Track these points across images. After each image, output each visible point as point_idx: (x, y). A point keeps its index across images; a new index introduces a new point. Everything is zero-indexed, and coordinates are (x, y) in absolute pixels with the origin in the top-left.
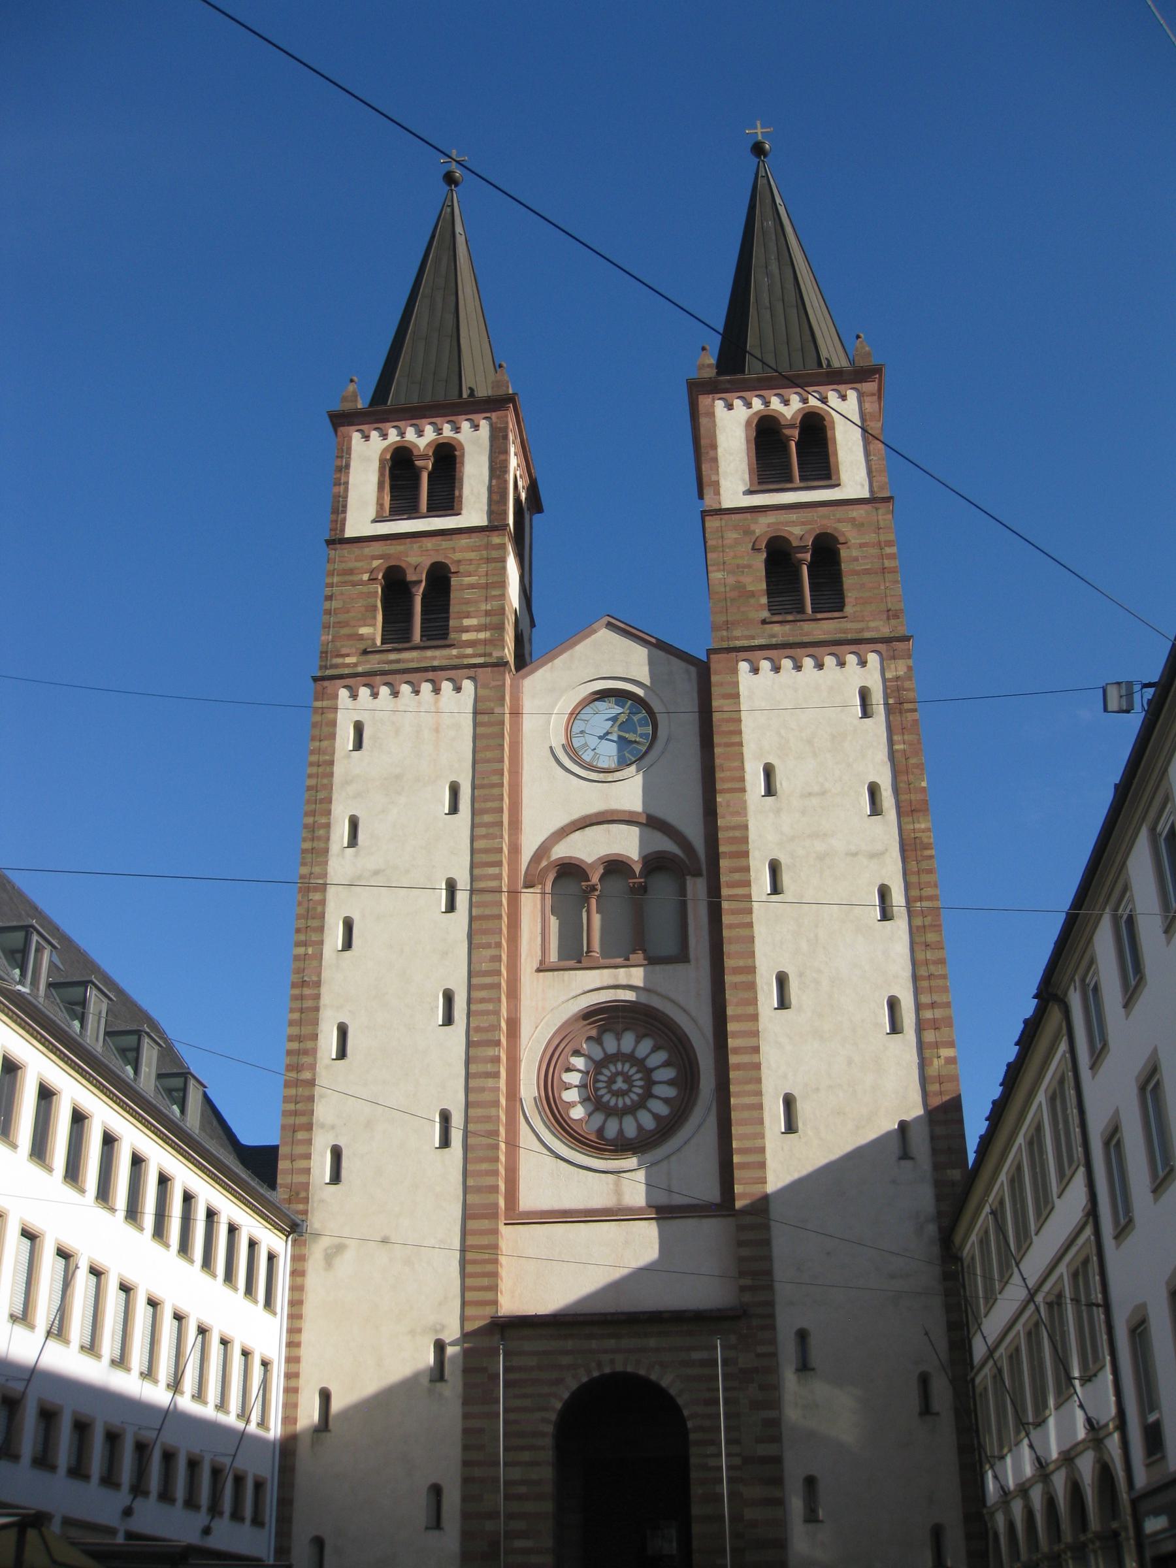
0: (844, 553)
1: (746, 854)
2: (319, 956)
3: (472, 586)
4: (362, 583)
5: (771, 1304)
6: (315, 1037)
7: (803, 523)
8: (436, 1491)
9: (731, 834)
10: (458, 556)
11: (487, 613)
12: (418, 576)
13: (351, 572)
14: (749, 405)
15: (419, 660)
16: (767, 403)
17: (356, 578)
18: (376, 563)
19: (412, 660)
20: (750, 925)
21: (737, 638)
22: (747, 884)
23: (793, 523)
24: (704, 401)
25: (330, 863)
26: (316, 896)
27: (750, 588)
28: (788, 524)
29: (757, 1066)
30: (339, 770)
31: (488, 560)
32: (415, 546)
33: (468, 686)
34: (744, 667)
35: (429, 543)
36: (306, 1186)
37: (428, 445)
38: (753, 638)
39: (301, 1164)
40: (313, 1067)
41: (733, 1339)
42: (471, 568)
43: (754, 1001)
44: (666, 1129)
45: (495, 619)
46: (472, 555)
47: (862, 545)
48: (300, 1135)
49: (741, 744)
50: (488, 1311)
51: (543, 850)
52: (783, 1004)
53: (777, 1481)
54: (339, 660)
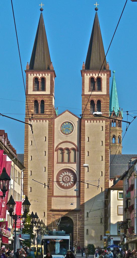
0: (101, 103)
2: (27, 161)
3: (48, 104)
4: (31, 102)
6: (27, 172)
7: (96, 98)
9: (83, 147)
10: (45, 99)
11: (50, 109)
12: (39, 102)
15: (40, 116)
16: (93, 75)
17: (30, 101)
18: (33, 99)
19: (39, 116)
21: (85, 117)
24: (83, 74)
25: (29, 148)
26: (27, 152)
31: (50, 100)
32: (39, 96)
33: (47, 121)
34: (86, 121)
35: (41, 96)
38: (87, 117)
39: (26, 189)
40: (27, 176)
41: (79, 213)
42: (47, 101)
43: (84, 171)
44: (73, 185)
45: (51, 110)
46: (48, 99)
47: (104, 102)
48: (26, 186)
50: (50, 208)
51: (57, 146)
53: (84, 230)
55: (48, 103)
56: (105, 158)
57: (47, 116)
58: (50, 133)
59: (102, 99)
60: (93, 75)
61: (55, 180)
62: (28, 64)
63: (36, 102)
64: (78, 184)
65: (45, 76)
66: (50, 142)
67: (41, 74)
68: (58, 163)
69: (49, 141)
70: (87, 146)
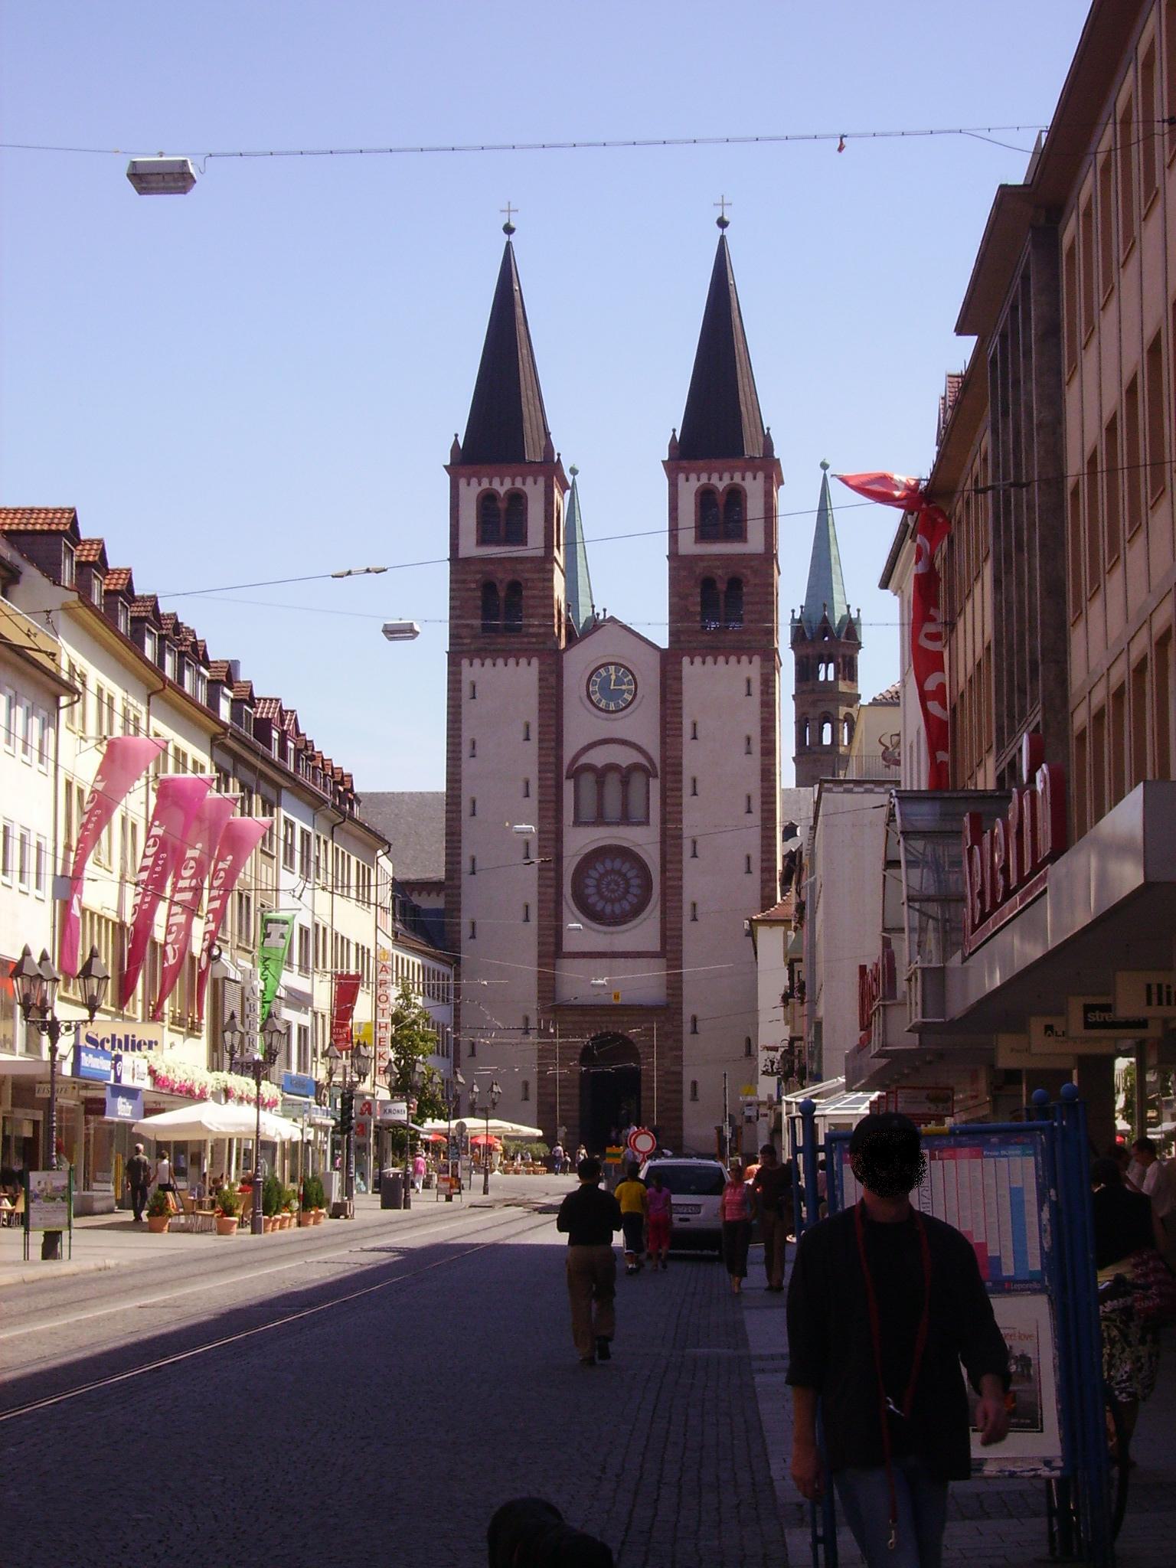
1: (680, 773)
3: (534, 597)
5: (681, 1003)
6: (459, 863)
8: (526, 1085)
10: (527, 575)
11: (544, 616)
13: (464, 582)
14: (699, 480)
16: (709, 479)
20: (681, 813)
22: (680, 790)
23: (718, 568)
27: (692, 609)
28: (718, 568)
29: (681, 887)
30: (464, 710)
33: (535, 661)
34: (686, 660)
36: (459, 940)
37: (506, 493)
46: (536, 576)
47: (755, 585)
49: (681, 708)
52: (695, 856)
53: (680, 1082)
54: (460, 641)
55: (535, 592)
56: (763, 803)
57: (533, 643)
58: (546, 707)
59: (748, 572)
60: (709, 479)
61: (567, 890)
62: (456, 441)
63: (489, 588)
64: (657, 903)
65: (523, 488)
66: (545, 745)
67: (508, 484)
68: (578, 822)
69: (540, 741)
70: (693, 759)
